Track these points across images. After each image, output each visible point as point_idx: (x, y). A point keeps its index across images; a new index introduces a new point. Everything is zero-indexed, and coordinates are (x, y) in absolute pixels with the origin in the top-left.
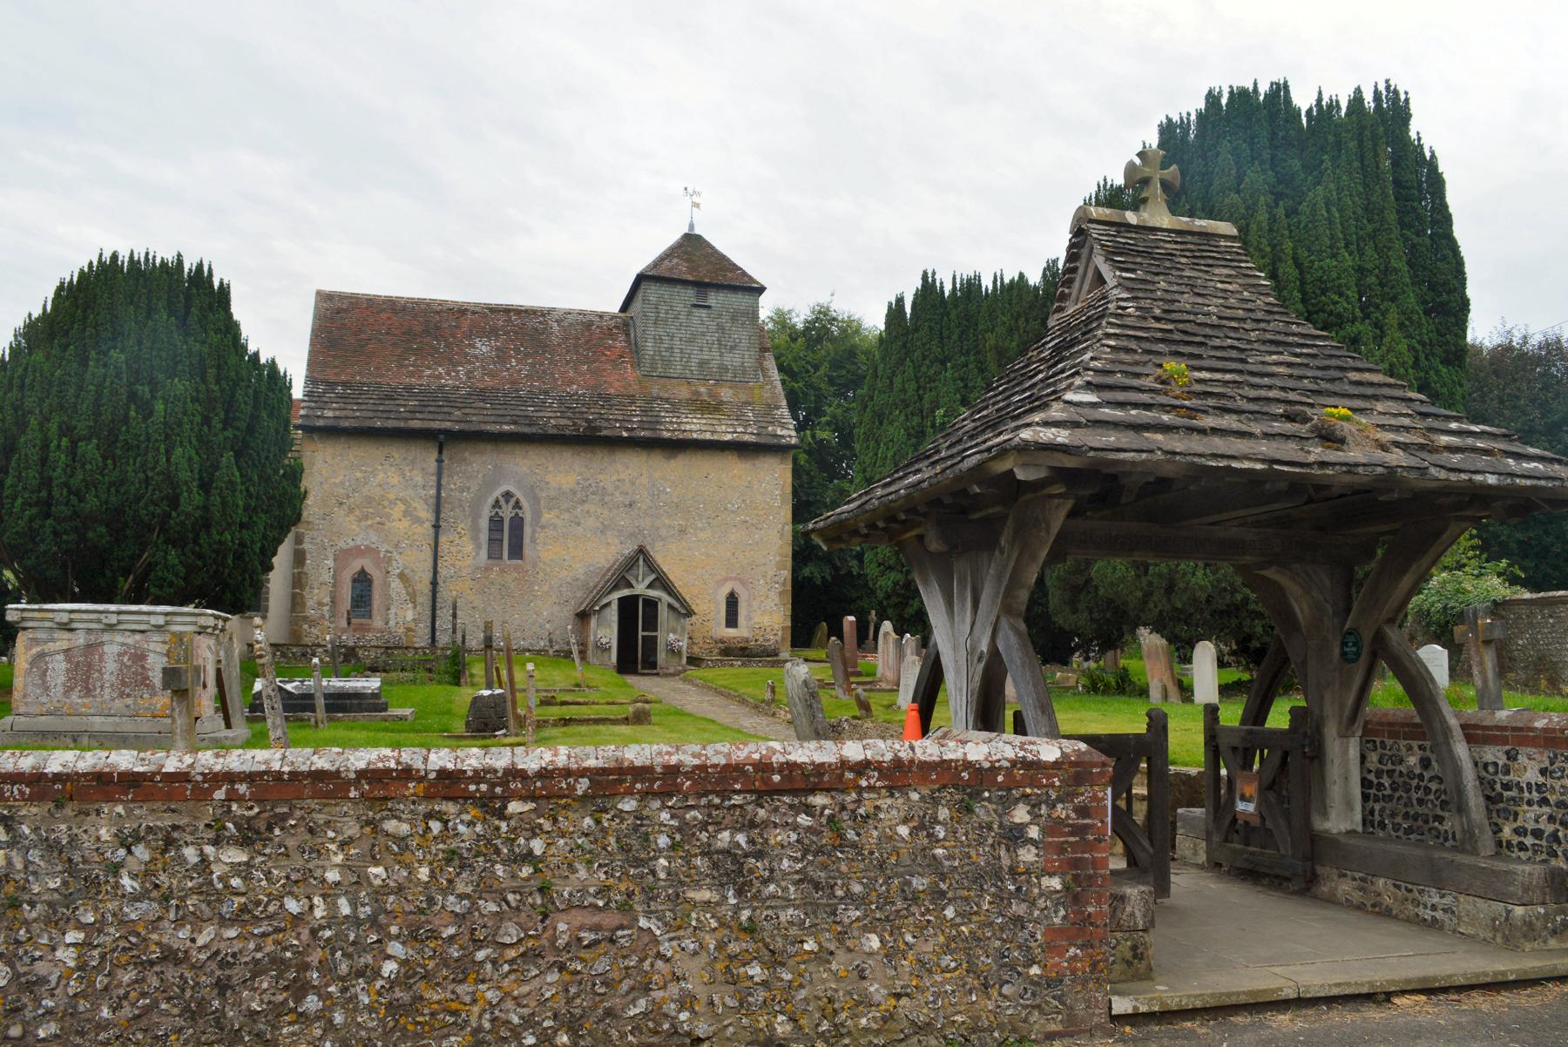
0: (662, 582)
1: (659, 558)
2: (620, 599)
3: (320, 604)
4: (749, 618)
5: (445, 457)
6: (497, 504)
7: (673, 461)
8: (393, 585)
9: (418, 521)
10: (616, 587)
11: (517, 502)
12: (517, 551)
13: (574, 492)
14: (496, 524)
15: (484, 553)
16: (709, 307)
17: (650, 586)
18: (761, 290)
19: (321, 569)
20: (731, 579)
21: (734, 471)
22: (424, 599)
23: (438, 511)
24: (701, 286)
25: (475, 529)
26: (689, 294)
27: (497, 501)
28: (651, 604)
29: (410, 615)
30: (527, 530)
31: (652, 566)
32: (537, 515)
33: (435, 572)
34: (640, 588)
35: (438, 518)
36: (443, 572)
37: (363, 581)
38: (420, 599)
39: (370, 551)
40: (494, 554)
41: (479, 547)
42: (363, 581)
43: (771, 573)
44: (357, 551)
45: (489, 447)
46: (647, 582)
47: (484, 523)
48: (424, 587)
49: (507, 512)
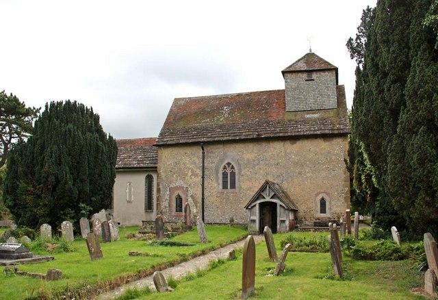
3: (166, 207)
4: (330, 209)
6: (225, 168)
9: (196, 175)
11: (233, 166)
12: (233, 186)
13: (254, 161)
14: (225, 175)
15: (221, 187)
16: (313, 80)
17: (272, 198)
19: (166, 195)
20: (322, 192)
22: (200, 205)
23: (203, 172)
26: (305, 76)
29: (195, 211)
30: (237, 177)
32: (240, 170)
34: (268, 199)
35: (203, 175)
36: (206, 194)
37: (179, 200)
39: (181, 188)
40: (225, 187)
42: (179, 200)
43: (340, 189)
44: (177, 188)
45: (221, 146)
46: (270, 196)
47: (220, 176)
49: (229, 171)
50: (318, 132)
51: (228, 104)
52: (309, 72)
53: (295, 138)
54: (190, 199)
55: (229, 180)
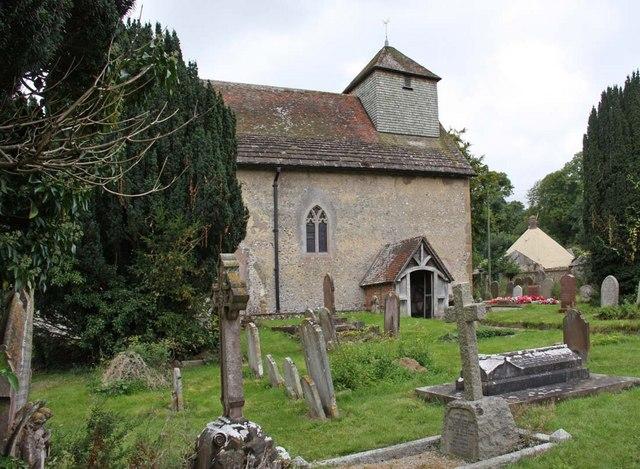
0: (435, 262)
1: (434, 244)
2: (411, 273)
5: (279, 183)
6: (311, 215)
7: (409, 186)
8: (251, 272)
9: (263, 227)
10: (408, 266)
11: (323, 213)
12: (324, 247)
14: (310, 227)
15: (305, 248)
18: (438, 79)
21: (438, 190)
22: (271, 281)
23: (276, 221)
24: (408, 76)
25: (299, 232)
26: (401, 81)
27: (311, 213)
28: (429, 274)
29: (262, 293)
30: (330, 232)
31: (428, 251)
32: (335, 220)
33: (277, 263)
35: (276, 225)
36: (281, 262)
38: (268, 281)
40: (311, 248)
41: (302, 244)
45: (305, 176)
47: (304, 229)
48: (270, 273)
49: (317, 221)
50: (442, 169)
51: (282, 105)
52: (408, 76)
53: (409, 175)
54: (253, 272)
55: (318, 238)
